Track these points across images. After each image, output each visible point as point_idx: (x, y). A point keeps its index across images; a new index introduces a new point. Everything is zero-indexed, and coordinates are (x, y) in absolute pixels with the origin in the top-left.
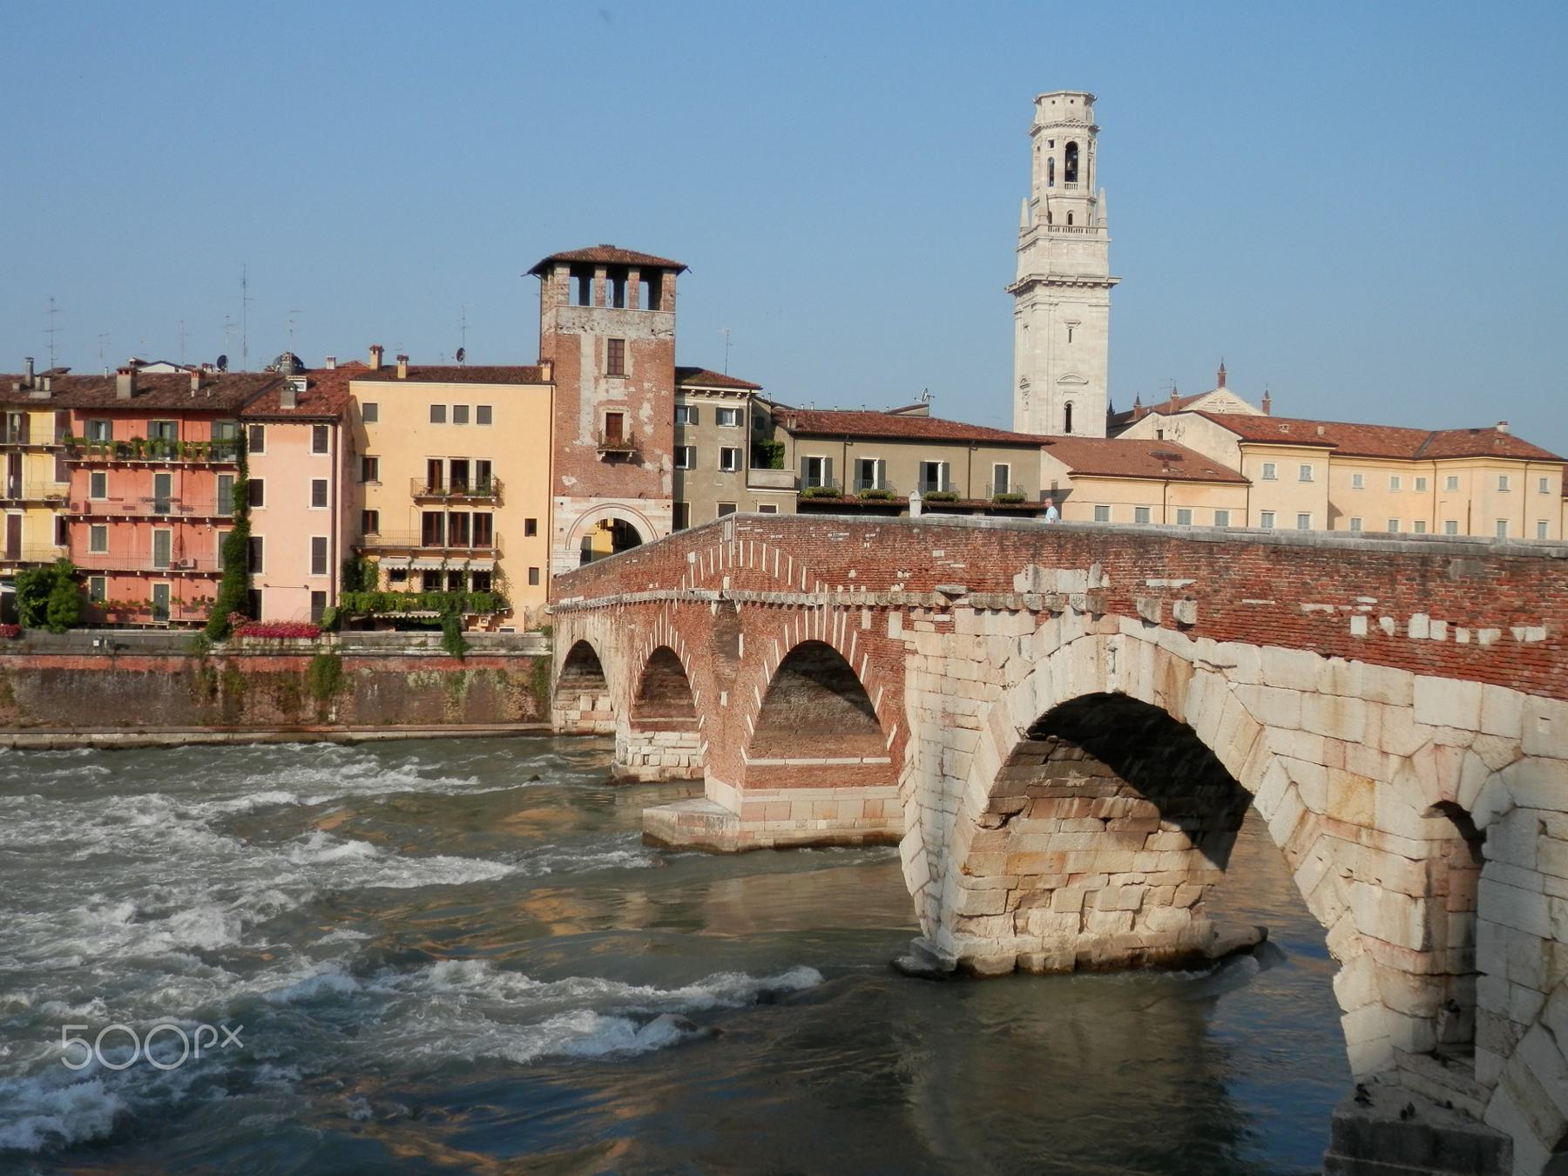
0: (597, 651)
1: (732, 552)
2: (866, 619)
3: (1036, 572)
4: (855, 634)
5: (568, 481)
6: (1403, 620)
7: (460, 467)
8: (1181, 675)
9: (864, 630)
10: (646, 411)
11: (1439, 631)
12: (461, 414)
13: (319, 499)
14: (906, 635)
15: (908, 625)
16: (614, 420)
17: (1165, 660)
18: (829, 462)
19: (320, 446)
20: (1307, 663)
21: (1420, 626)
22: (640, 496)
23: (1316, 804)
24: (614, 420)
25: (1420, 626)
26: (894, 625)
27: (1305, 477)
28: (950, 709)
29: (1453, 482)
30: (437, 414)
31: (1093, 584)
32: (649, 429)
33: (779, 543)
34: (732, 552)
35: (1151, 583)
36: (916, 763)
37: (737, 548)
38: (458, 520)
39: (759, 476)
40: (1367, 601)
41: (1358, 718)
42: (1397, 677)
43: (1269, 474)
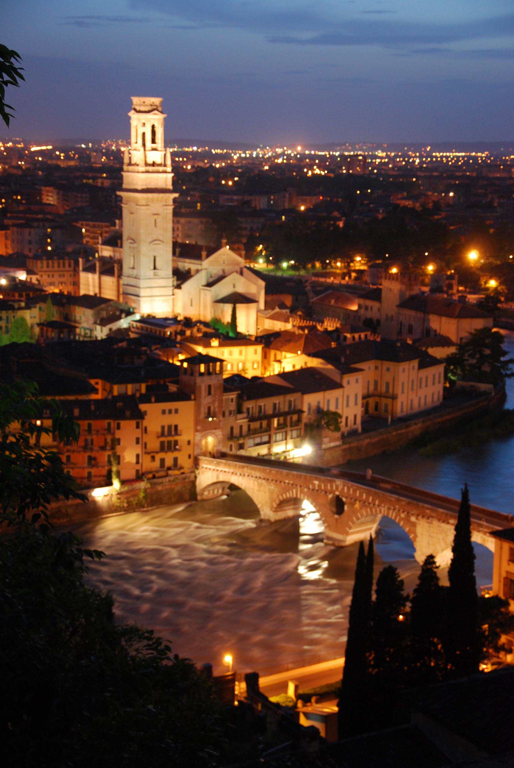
1: (340, 488)
5: (199, 428)
7: (170, 427)
10: (216, 404)
12: (170, 412)
13: (138, 442)
15: (417, 519)
16: (209, 408)
18: (252, 408)
19: (138, 427)
22: (216, 429)
24: (209, 408)
27: (357, 381)
29: (388, 369)
30: (164, 412)
32: (217, 410)
34: (340, 488)
37: (343, 489)
38: (169, 442)
39: (240, 416)
43: (348, 383)
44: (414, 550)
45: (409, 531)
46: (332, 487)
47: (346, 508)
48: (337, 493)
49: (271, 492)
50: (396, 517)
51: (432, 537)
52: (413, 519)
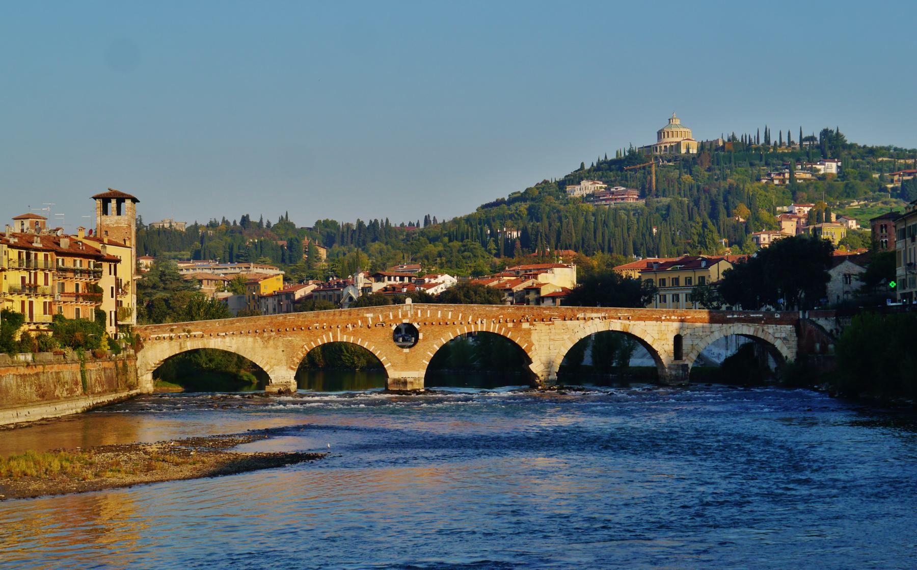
0: (232, 350)
2: (510, 325)
3: (585, 314)
4: (504, 329)
6: (670, 316)
8: (627, 326)
9: (509, 328)
11: (676, 318)
14: (532, 327)
17: (623, 325)
20: (655, 322)
21: (673, 317)
23: (656, 338)
25: (673, 317)
26: (525, 325)
28: (552, 338)
31: (603, 315)
33: (452, 311)
35: (619, 315)
36: (537, 347)
40: (665, 315)
41: (663, 328)
42: (670, 323)
44: (530, 362)
45: (520, 341)
46: (395, 317)
47: (421, 336)
48: (406, 321)
49: (290, 346)
50: (500, 329)
51: (553, 340)
52: (525, 325)
